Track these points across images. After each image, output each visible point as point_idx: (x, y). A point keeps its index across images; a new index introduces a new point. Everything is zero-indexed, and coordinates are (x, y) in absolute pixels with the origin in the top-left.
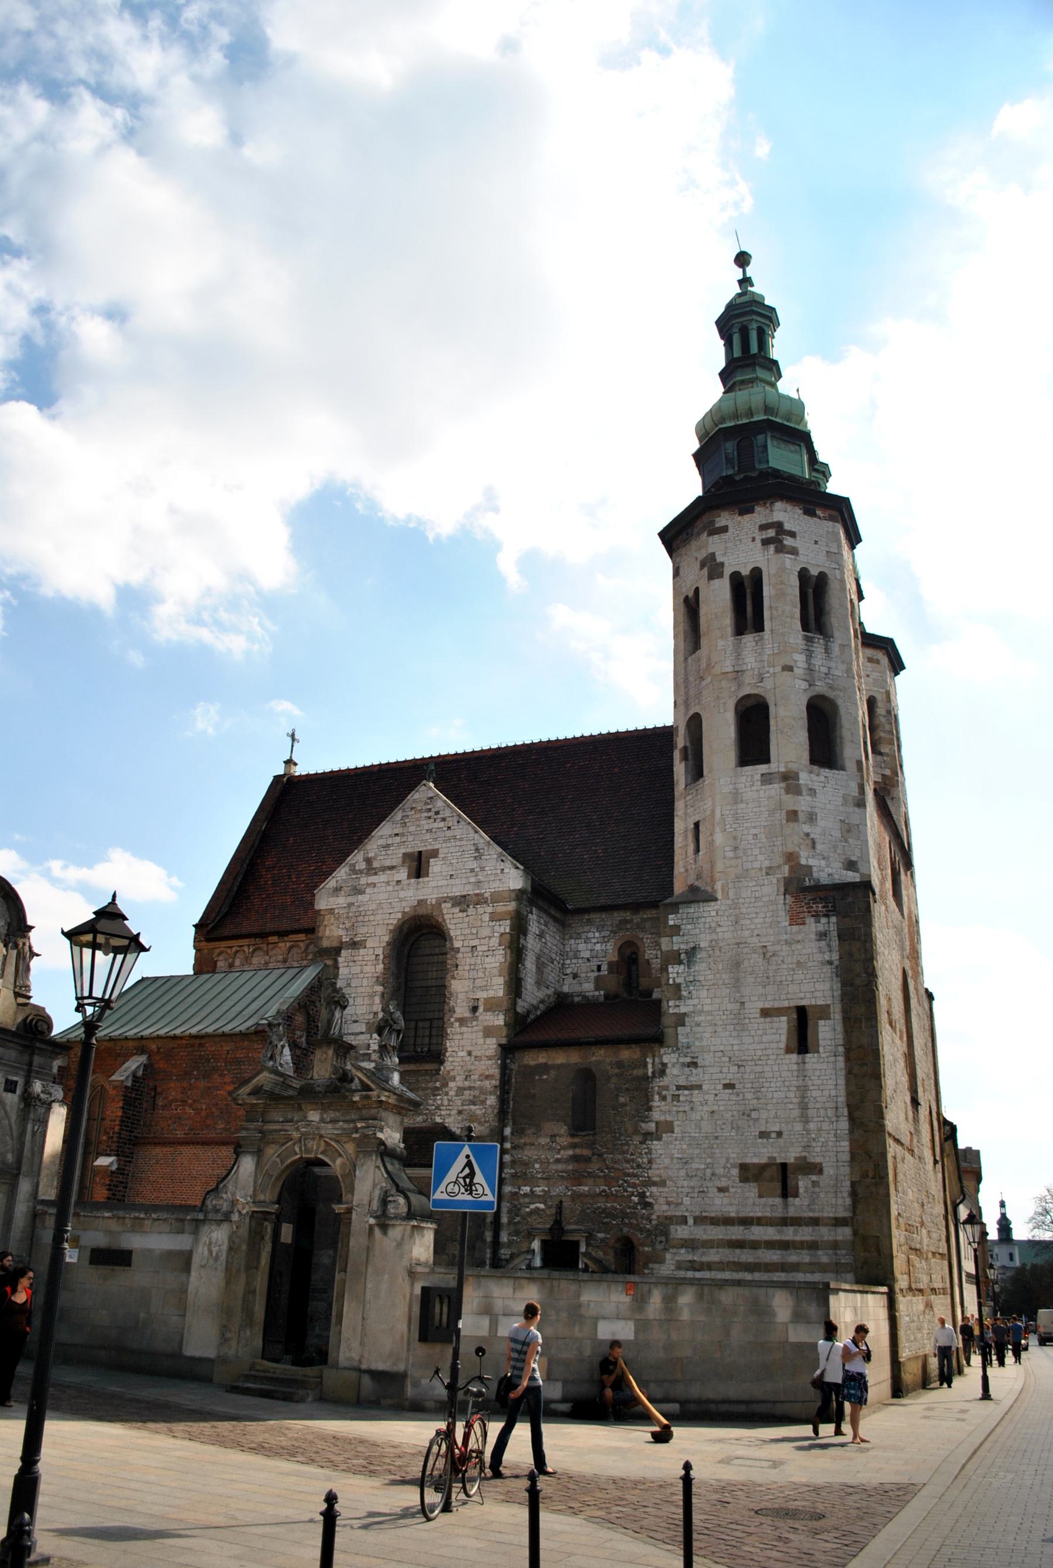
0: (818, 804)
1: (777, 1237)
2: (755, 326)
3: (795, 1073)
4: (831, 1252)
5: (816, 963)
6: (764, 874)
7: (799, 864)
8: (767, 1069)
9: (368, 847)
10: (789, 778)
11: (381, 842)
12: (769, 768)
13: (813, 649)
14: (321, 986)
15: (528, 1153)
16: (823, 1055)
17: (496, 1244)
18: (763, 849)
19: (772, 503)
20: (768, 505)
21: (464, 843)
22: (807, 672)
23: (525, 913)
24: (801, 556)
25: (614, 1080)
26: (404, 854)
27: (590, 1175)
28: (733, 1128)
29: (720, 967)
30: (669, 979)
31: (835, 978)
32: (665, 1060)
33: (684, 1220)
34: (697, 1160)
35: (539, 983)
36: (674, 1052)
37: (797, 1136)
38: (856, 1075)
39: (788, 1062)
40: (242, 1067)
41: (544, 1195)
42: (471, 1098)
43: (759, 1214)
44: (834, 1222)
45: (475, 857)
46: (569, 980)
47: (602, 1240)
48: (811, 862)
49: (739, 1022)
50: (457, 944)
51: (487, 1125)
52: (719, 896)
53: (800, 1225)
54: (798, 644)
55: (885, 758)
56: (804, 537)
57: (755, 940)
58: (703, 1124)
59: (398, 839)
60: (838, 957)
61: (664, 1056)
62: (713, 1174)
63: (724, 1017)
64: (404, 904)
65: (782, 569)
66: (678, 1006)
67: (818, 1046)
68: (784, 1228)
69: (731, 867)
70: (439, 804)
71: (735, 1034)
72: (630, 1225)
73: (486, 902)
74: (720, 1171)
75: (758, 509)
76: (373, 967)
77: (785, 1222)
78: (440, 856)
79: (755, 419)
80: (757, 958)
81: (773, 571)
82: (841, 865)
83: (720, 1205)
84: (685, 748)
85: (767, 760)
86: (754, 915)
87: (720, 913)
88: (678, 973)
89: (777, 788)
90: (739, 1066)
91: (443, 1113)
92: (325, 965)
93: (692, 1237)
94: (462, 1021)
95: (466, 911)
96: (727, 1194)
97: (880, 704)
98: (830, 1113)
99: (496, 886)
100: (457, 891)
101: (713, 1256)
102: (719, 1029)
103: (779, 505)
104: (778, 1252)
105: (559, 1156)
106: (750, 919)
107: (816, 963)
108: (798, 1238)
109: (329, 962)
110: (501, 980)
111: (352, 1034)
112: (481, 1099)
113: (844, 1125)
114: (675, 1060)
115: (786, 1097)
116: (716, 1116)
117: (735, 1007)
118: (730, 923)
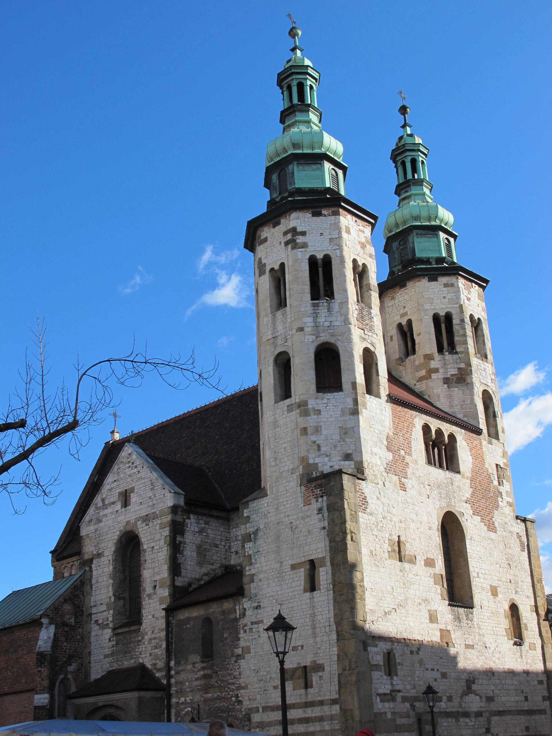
0: (322, 420)
1: (303, 716)
2: (294, 84)
4: (330, 722)
5: (317, 530)
6: (290, 474)
8: (295, 604)
9: (103, 491)
11: (108, 487)
12: (291, 401)
13: (318, 311)
14: (83, 585)
15: (183, 676)
16: (322, 591)
19: (290, 215)
20: (288, 217)
21: (146, 480)
23: (182, 520)
24: (309, 247)
25: (221, 623)
26: (120, 493)
27: (212, 686)
29: (270, 540)
30: (245, 552)
31: (327, 539)
32: (245, 607)
33: (257, 710)
35: (200, 564)
36: (249, 600)
38: (338, 602)
39: (304, 598)
40: (31, 643)
41: (191, 702)
42: (155, 644)
43: (294, 702)
45: (151, 488)
46: (234, 556)
48: (317, 460)
50: (145, 547)
52: (269, 494)
53: (314, 706)
54: (306, 311)
55: (460, 356)
57: (287, 519)
59: (116, 483)
60: (327, 524)
61: (245, 604)
63: (273, 573)
64: (120, 525)
66: (250, 570)
67: (320, 585)
69: (274, 472)
70: (134, 457)
71: (278, 584)
72: (232, 715)
75: (282, 221)
78: (136, 491)
79: (289, 153)
81: (290, 263)
82: (340, 458)
87: (269, 504)
88: (249, 548)
89: (295, 413)
91: (143, 656)
92: (85, 570)
93: (262, 720)
94: (149, 596)
97: (454, 317)
98: (327, 628)
102: (271, 581)
103: (294, 215)
104: (305, 725)
105: (197, 676)
106: (284, 505)
107: (317, 530)
108: (314, 715)
109: (87, 569)
111: (100, 612)
112: (160, 644)
113: (334, 636)
114: (249, 606)
117: (277, 565)
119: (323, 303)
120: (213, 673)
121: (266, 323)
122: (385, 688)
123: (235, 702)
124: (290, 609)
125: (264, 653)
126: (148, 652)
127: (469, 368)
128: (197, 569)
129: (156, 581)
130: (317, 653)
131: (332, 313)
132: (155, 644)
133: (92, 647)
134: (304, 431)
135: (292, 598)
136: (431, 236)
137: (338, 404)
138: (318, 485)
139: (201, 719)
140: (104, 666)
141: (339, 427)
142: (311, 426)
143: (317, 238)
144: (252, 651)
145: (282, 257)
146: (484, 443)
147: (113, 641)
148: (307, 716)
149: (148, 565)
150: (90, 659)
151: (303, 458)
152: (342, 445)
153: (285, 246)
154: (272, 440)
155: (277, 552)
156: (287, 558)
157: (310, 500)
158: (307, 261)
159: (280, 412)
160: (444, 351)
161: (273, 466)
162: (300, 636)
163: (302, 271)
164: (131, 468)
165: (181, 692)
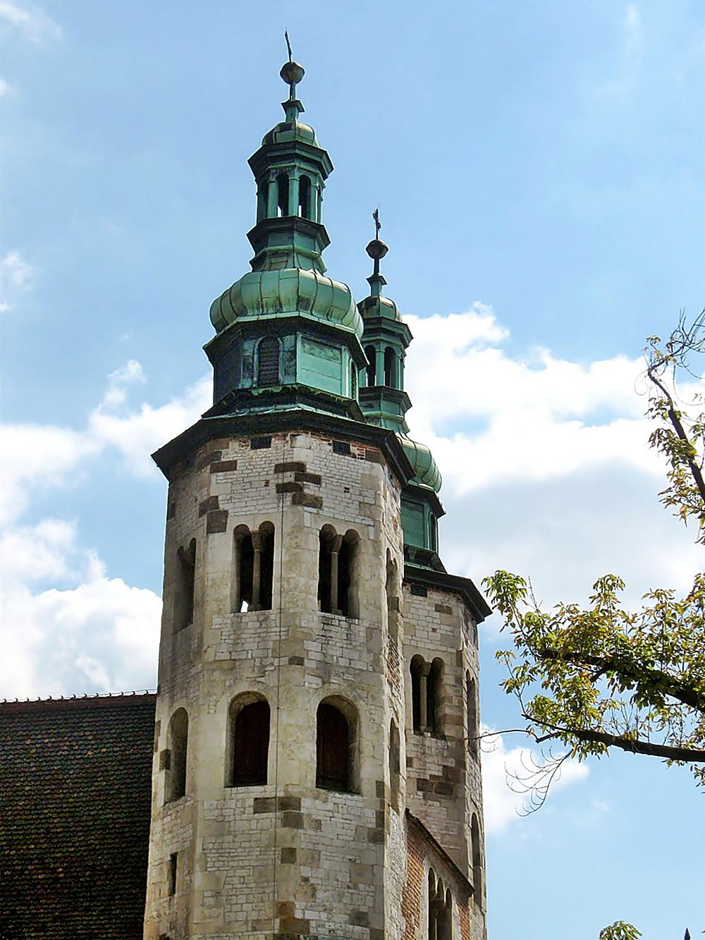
2: (297, 175)
6: (250, 929)
7: (294, 918)
10: (288, 807)
18: (251, 897)
20: (288, 438)
65: (299, 528)
84: (166, 754)
85: (262, 780)
97: (447, 670)
103: (303, 439)
119: (339, 621)
121: (218, 626)
127: (462, 771)
136: (413, 505)
141: (350, 860)
142: (303, 849)
143: (339, 494)
145: (270, 511)
151: (284, 905)
153: (278, 492)
154: (211, 855)
160: (423, 728)
161: (211, 907)
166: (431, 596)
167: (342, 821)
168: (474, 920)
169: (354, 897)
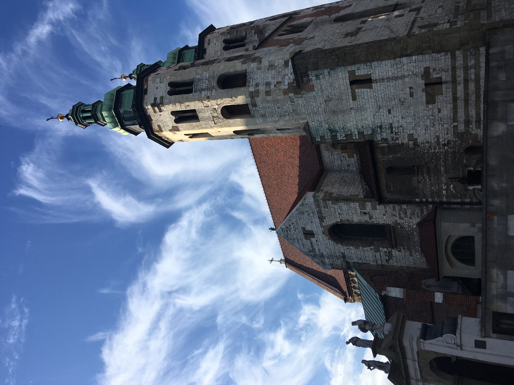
1: (462, 85)
3: (381, 83)
6: (294, 103)
10: (253, 95)
16: (372, 72)
17: (471, 203)
21: (298, 218)
22: (208, 90)
26: (305, 239)
28: (409, 109)
29: (336, 119)
32: (379, 139)
33: (455, 127)
34: (426, 123)
37: (411, 80)
38: (380, 56)
39: (376, 87)
42: (404, 214)
43: (451, 94)
44: (453, 59)
47: (467, 161)
48: (286, 83)
49: (360, 109)
50: (339, 220)
51: (415, 208)
52: (306, 121)
56: (156, 94)
58: (408, 121)
59: (300, 241)
61: (378, 139)
62: (432, 116)
63: (358, 116)
64: (325, 239)
66: (355, 136)
68: (457, 82)
71: (365, 111)
73: (320, 210)
74: (431, 112)
76: (352, 250)
77: (454, 82)
80: (330, 104)
82: (287, 69)
83: (447, 112)
86: (312, 106)
87: (313, 120)
88: (341, 136)
90: (380, 108)
91: (412, 225)
94: (371, 218)
95: (325, 217)
96: (441, 109)
97: (226, 38)
98: (398, 66)
99: (313, 206)
100: (317, 220)
101: (473, 113)
102: (364, 118)
104: (470, 83)
105: (428, 180)
108: (462, 76)
110: (352, 204)
111: (381, 258)
112: (404, 210)
113: (405, 60)
115: (393, 86)
116: (404, 116)
118: (317, 116)
120: (426, 166)
122: (447, 26)
123: (448, 146)
124: (383, 100)
125: (413, 122)
126: (409, 220)
128: (356, 186)
129: (361, 212)
130: (416, 75)
131: (201, 79)
132: (404, 214)
133: (405, 265)
134: (268, 93)
135: (375, 99)
137: (254, 72)
138: (301, 79)
139: (460, 177)
140: (418, 257)
141: (268, 70)
142: (265, 89)
144: (412, 132)
146: (298, 16)
147: (400, 248)
148: (462, 82)
149: (350, 218)
150: (412, 268)
152: (278, 68)
153: (162, 111)
155: (344, 113)
156: (348, 104)
157: (311, 85)
158: (170, 96)
159: (256, 113)
160: (244, 43)
162: (402, 90)
163: (175, 99)
164: (291, 229)
165: (439, 193)
166: (206, 47)
167: (255, 75)
168: (301, 14)
169: (279, 67)
